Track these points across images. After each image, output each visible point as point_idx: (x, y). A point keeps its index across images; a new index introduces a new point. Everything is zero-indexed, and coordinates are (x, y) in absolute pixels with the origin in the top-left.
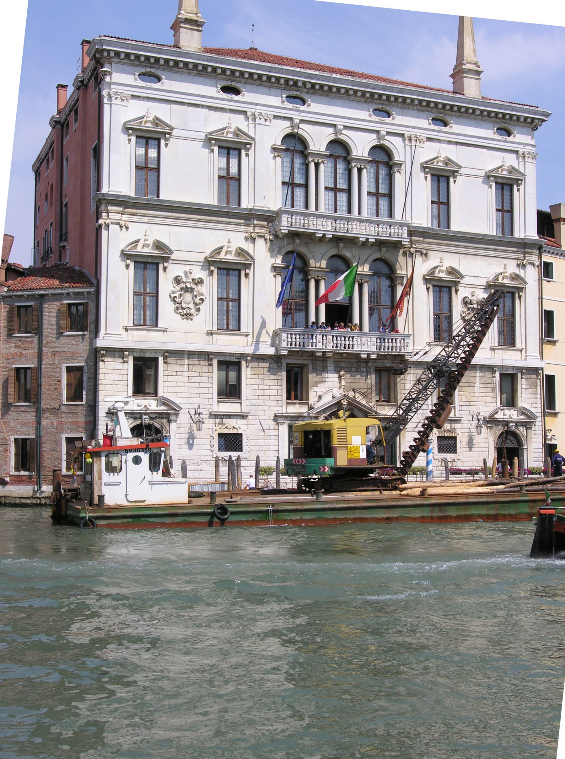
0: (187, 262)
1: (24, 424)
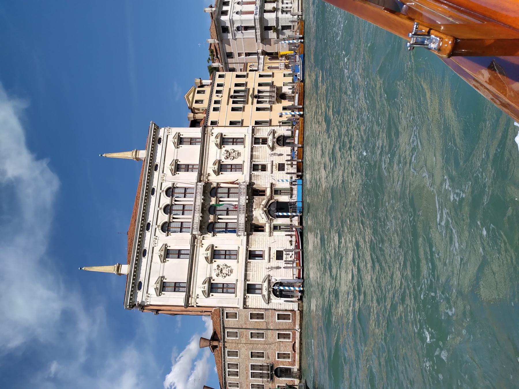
1: (272, 335)
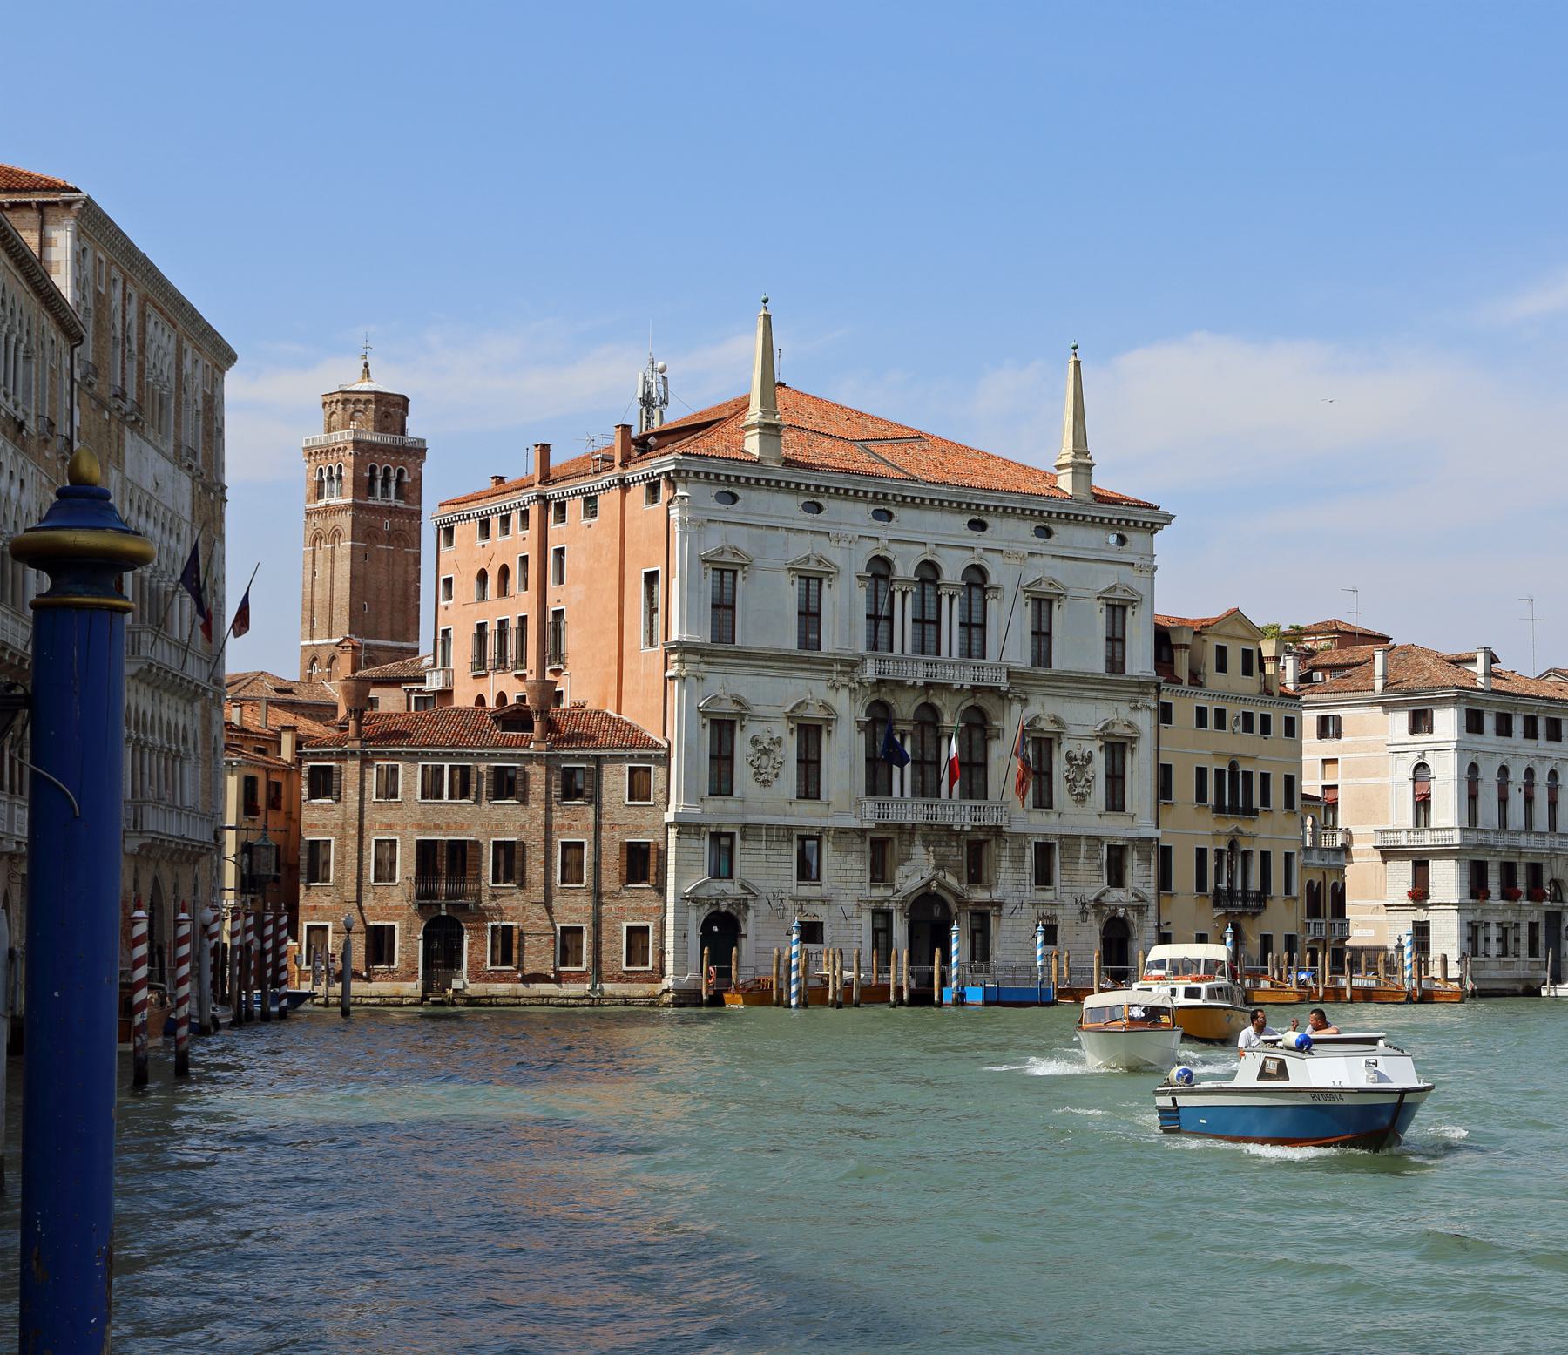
0: (766, 719)
1: (575, 910)
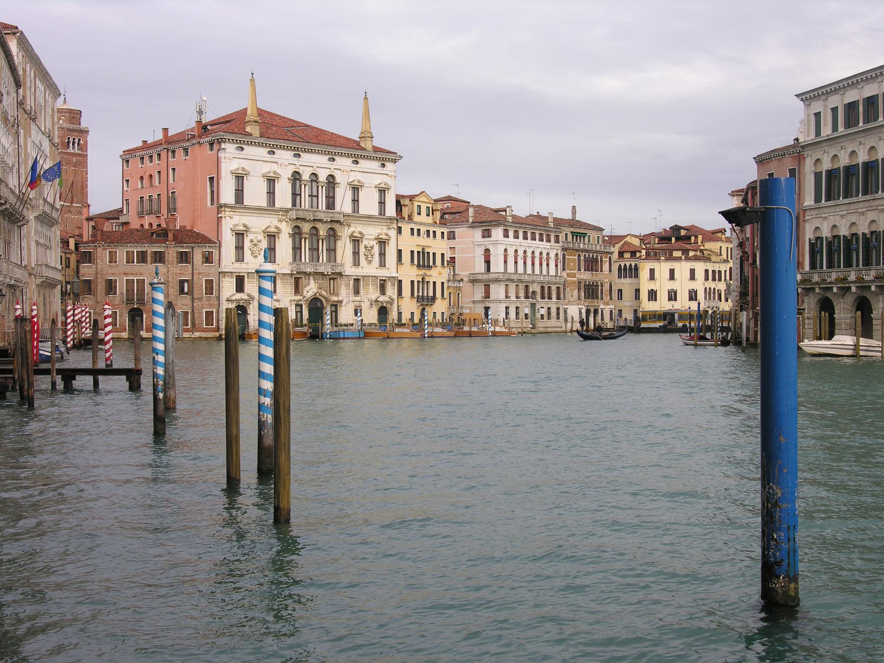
0: (255, 233)
